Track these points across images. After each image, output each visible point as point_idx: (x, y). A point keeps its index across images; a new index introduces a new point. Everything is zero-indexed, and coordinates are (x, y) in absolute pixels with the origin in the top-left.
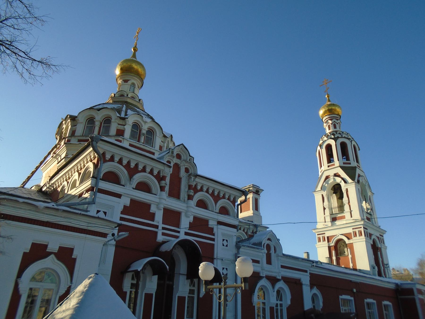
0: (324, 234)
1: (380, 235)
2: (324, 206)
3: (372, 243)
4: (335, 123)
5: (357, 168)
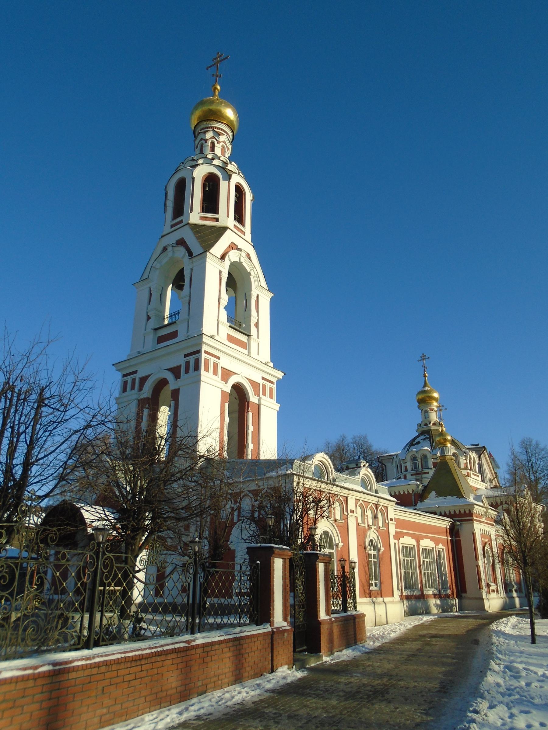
0: (135, 372)
1: (263, 378)
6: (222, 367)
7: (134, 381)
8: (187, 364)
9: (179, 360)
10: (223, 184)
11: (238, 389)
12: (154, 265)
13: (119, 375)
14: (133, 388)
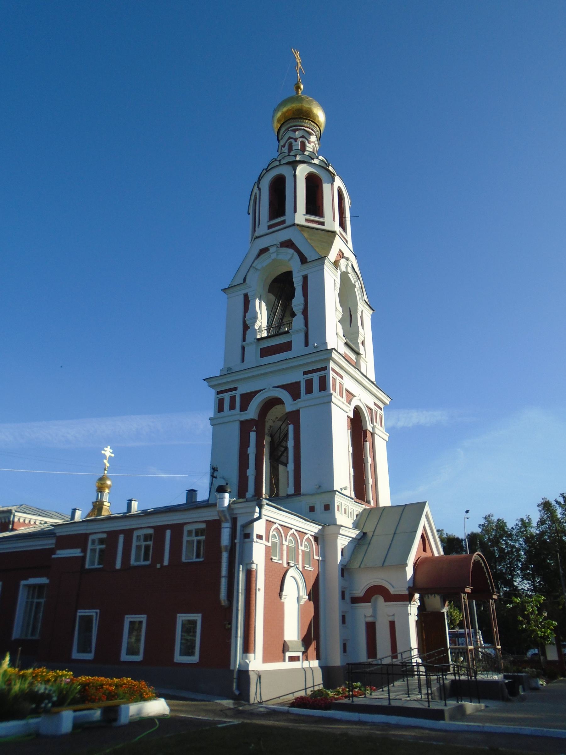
0: (235, 389)
3: (352, 417)
4: (304, 139)
5: (337, 235)
7: (233, 399)
9: (297, 376)
10: (326, 187)
11: (357, 411)
13: (213, 392)
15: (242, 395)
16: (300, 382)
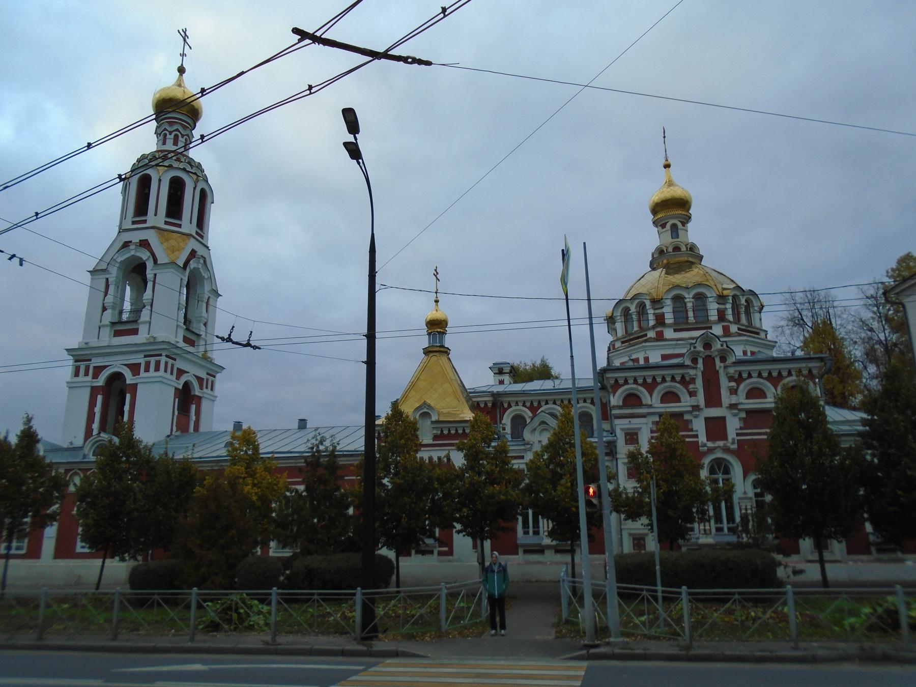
2: (104, 304)
6: (178, 369)
8: (148, 365)
11: (187, 385)
12: (114, 258)
14: (86, 374)
15: (95, 367)
16: (140, 363)
